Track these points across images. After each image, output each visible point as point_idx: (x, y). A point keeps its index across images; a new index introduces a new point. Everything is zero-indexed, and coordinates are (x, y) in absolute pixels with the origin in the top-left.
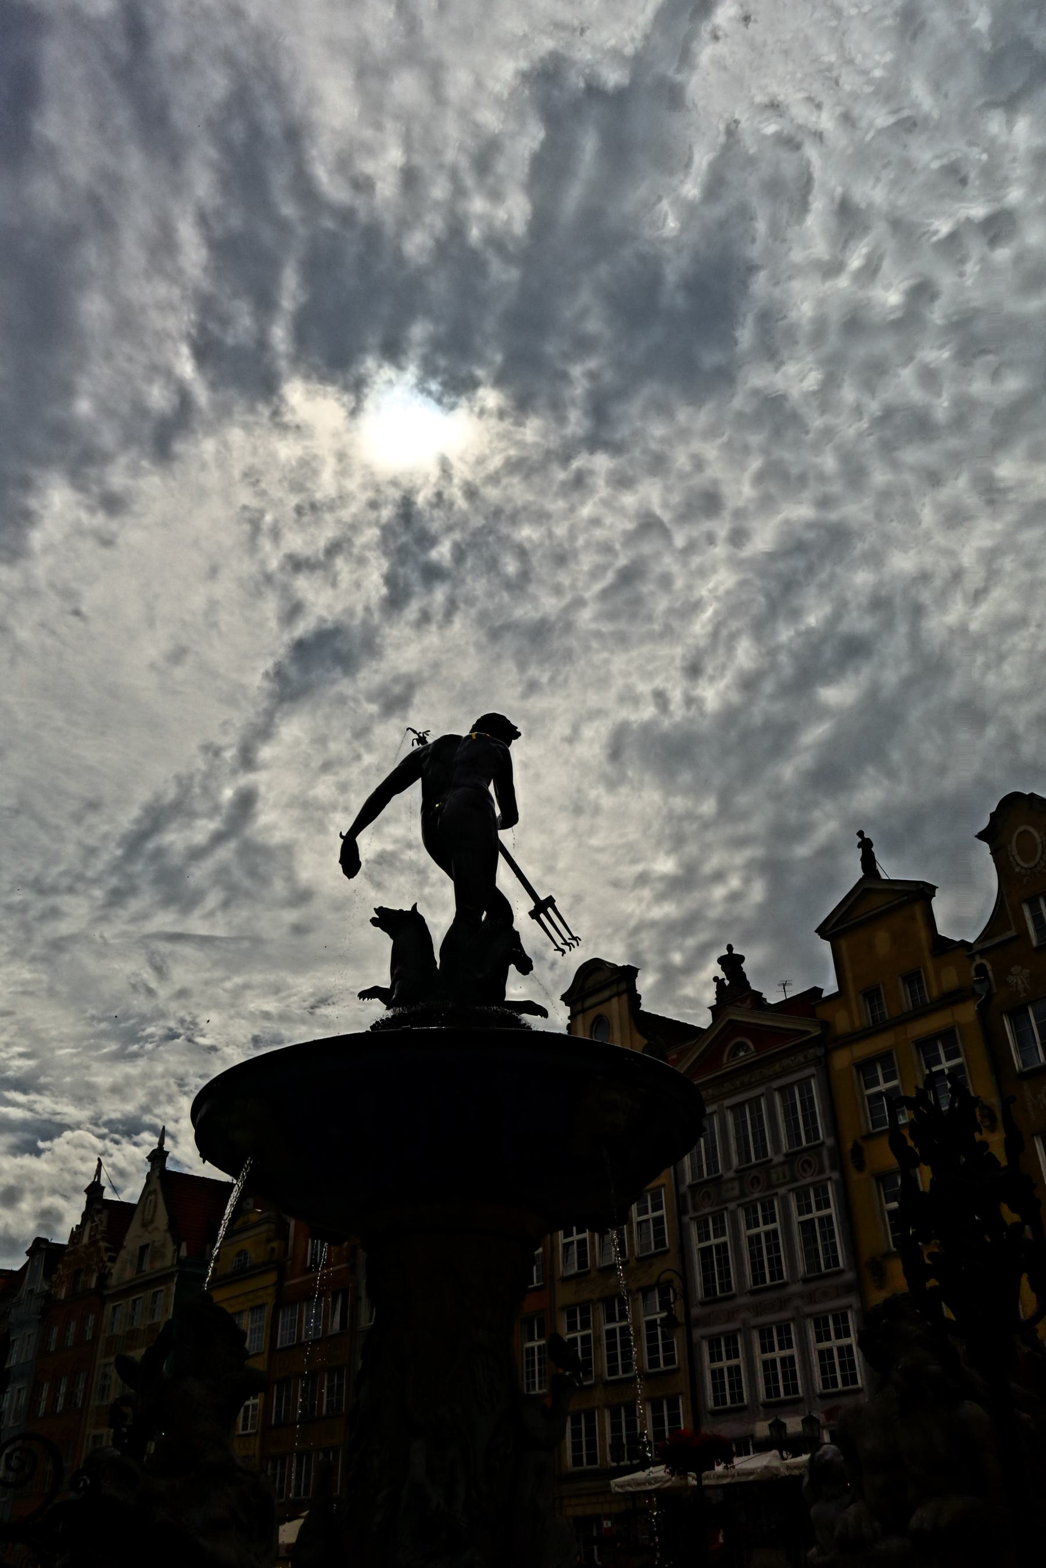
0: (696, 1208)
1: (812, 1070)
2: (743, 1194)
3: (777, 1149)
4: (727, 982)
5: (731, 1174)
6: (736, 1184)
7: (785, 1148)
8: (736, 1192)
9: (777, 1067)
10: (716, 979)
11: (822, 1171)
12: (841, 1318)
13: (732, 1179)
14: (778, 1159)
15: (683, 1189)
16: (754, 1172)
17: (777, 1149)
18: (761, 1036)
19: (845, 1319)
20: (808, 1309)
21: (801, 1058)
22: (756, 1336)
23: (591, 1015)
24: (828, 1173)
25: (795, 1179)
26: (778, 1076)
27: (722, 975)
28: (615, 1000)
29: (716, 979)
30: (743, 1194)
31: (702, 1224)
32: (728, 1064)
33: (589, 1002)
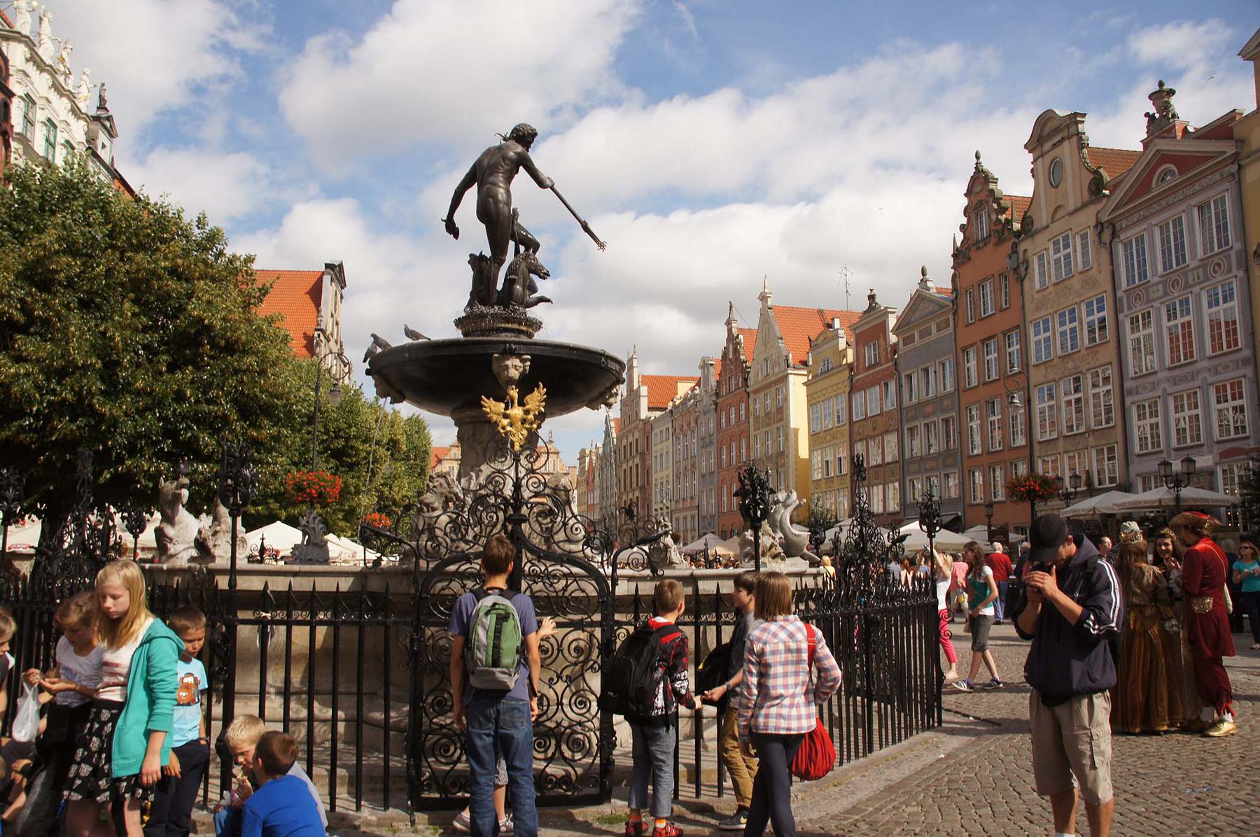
0: (1130, 308)
1: (1227, 185)
2: (1166, 294)
3: (1193, 257)
4: (1157, 116)
5: (1157, 279)
6: (1160, 287)
7: (1200, 254)
8: (1161, 293)
9: (1197, 187)
10: (1147, 115)
11: (1229, 271)
12: (1236, 385)
13: (1157, 284)
14: (1194, 264)
15: (1119, 293)
16: (1175, 276)
17: (1193, 257)
18: (1184, 162)
19: (1240, 386)
20: (1210, 379)
21: (1217, 177)
22: (1171, 401)
23: (1048, 158)
24: (1235, 272)
25: (1207, 279)
26: (1195, 194)
27: (1152, 110)
28: (1066, 143)
29: (1147, 115)
30: (1166, 294)
31: (1134, 321)
32: (1156, 188)
33: (1047, 146)
